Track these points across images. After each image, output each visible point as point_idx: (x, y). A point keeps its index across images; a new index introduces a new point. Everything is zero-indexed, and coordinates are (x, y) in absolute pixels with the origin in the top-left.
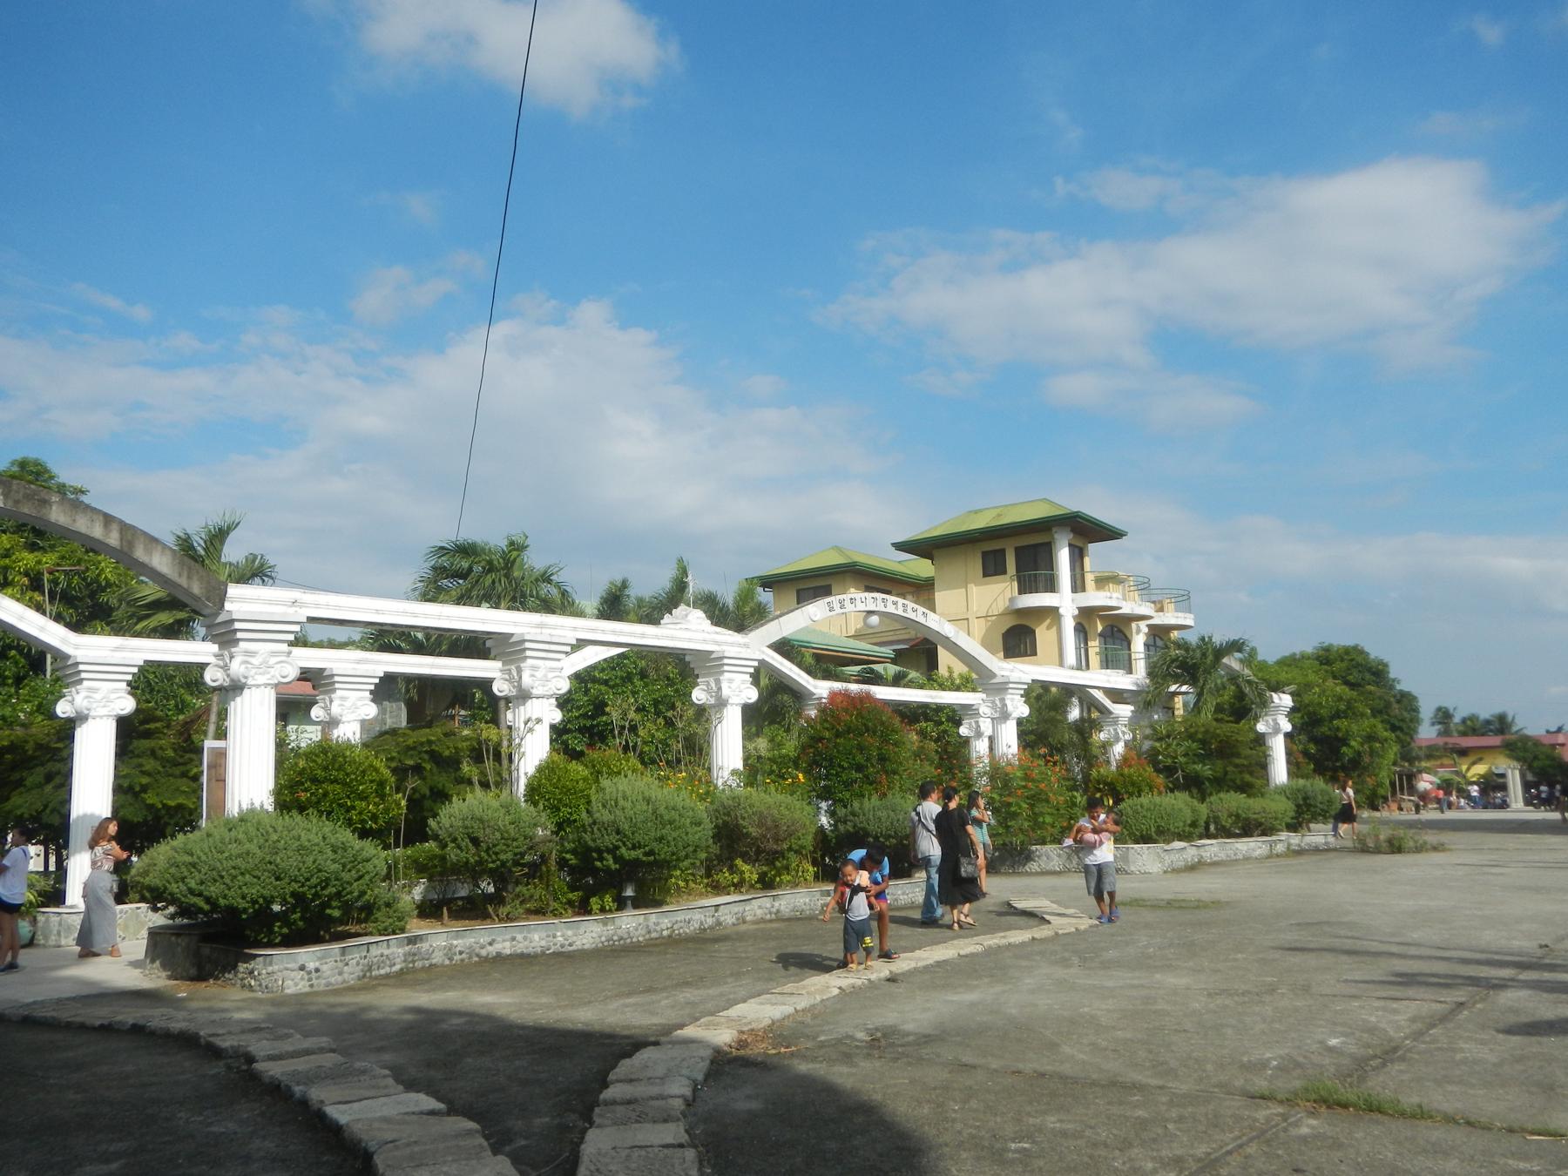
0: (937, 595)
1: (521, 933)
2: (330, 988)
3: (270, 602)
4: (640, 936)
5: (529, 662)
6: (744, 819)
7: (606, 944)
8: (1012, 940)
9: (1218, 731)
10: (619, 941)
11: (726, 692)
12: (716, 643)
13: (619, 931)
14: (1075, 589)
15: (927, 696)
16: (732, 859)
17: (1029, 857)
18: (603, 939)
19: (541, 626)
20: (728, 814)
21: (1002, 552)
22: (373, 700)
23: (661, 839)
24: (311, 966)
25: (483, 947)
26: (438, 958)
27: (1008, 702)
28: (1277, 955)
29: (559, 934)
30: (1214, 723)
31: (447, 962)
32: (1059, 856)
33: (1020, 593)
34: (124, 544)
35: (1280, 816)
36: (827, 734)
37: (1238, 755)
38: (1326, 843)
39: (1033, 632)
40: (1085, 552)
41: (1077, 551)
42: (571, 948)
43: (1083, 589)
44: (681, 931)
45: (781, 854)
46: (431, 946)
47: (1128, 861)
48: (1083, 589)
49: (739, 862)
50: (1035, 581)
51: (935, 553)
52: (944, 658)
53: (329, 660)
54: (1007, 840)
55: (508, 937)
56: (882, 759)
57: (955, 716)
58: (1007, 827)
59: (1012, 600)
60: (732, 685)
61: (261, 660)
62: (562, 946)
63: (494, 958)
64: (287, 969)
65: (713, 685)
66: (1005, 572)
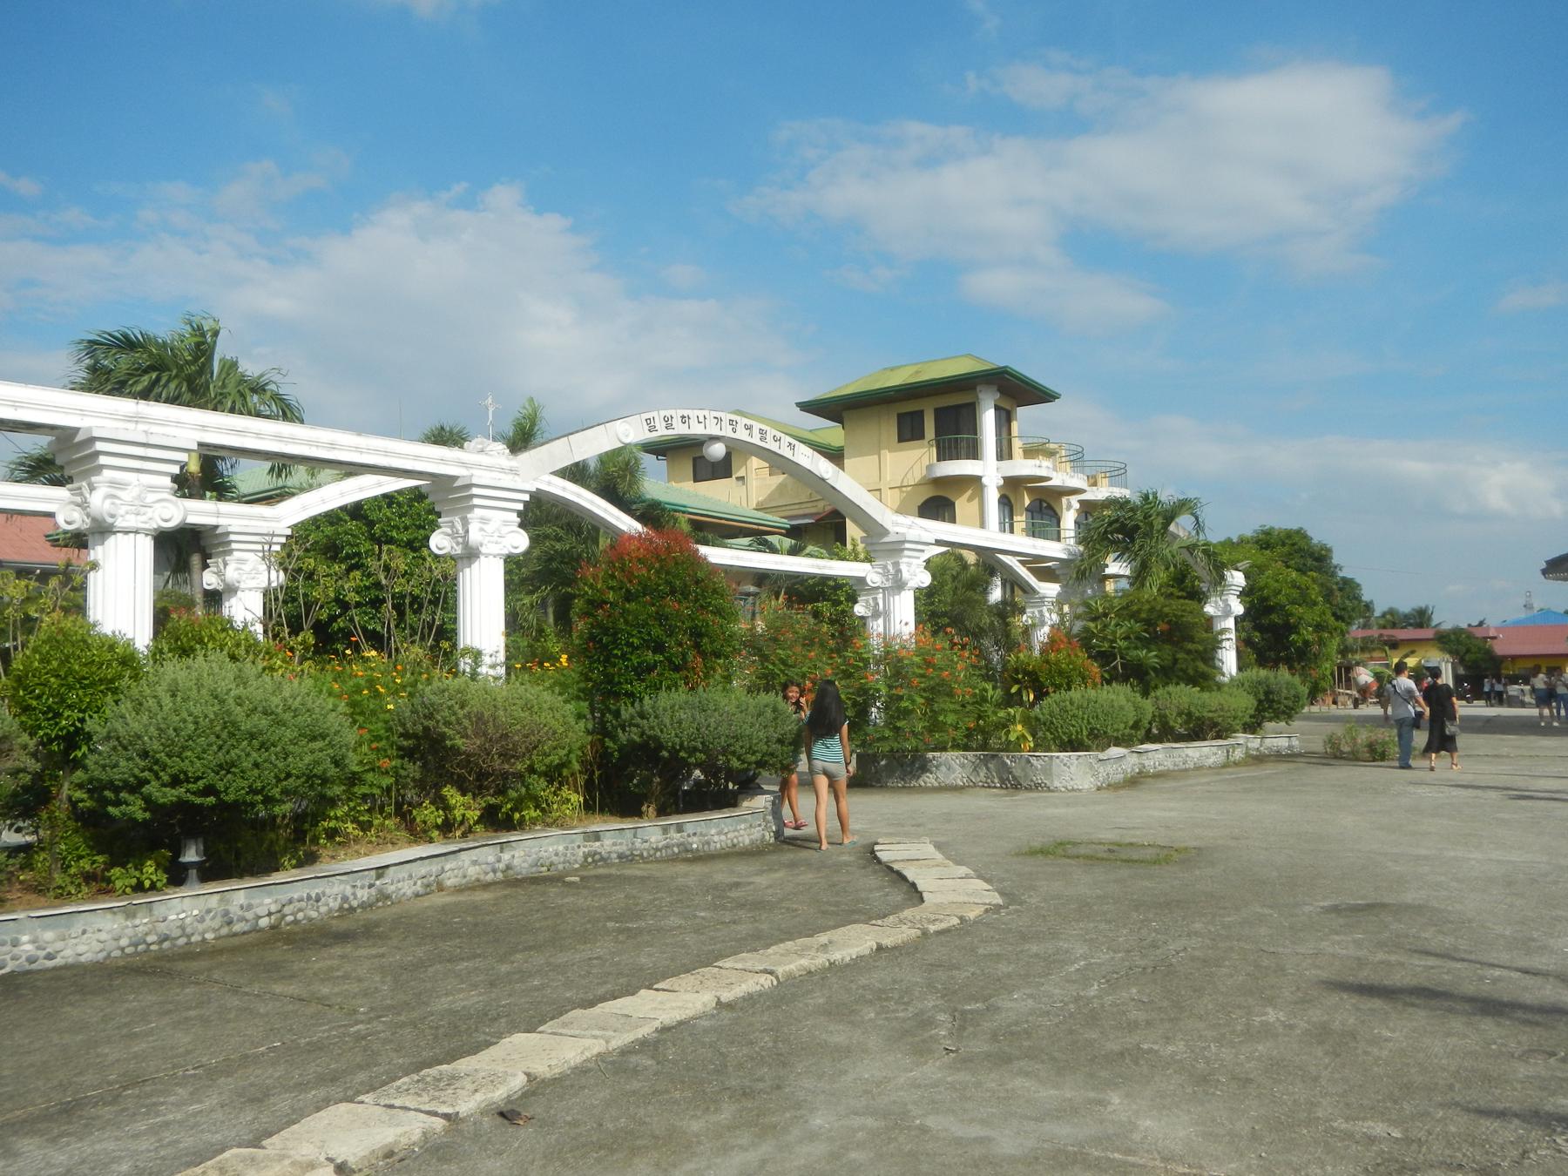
0: (846, 461)
5: (107, 473)
6: (448, 724)
7: (129, 950)
8: (837, 956)
9: (1166, 610)
10: (161, 942)
11: (475, 536)
12: (463, 464)
13: (162, 927)
14: (1000, 457)
15: (813, 566)
16: (438, 787)
17: (924, 768)
18: (124, 942)
19: (136, 419)
21: (920, 414)
23: (227, 767)
27: (903, 567)
28: (1344, 1012)
29: (25, 938)
30: (1161, 599)
32: (963, 766)
33: (938, 460)
35: (1240, 714)
36: (611, 596)
37: (1192, 640)
38: (1290, 747)
39: (954, 504)
40: (1013, 416)
41: (1004, 415)
42: (50, 964)
43: (1010, 457)
44: (300, 916)
47: (1051, 775)
48: (1010, 457)
49: (450, 792)
50: (956, 448)
51: (845, 414)
52: (853, 531)
54: (896, 745)
56: (697, 634)
57: (847, 591)
58: (897, 729)
59: (929, 467)
62: (32, 960)
65: (460, 528)
66: (922, 437)
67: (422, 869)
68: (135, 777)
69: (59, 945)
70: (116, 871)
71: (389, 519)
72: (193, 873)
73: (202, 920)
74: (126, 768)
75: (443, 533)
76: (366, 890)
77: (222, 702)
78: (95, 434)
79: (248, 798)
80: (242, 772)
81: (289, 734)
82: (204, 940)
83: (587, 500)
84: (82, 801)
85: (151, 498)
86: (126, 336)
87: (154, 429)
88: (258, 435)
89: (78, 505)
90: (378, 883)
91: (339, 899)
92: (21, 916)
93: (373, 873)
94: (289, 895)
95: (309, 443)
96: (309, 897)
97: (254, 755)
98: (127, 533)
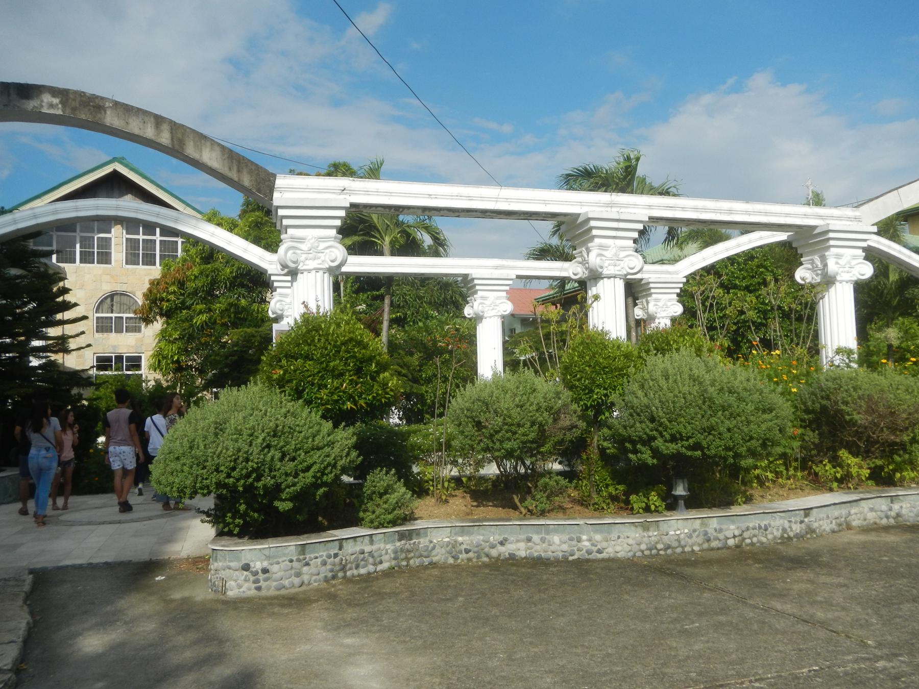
1: (538, 533)
2: (283, 592)
3: (319, 190)
4: (695, 545)
5: (597, 241)
6: (846, 403)
7: (647, 553)
10: (666, 549)
11: (832, 267)
12: (820, 217)
13: (665, 539)
16: (835, 450)
18: (643, 547)
19: (611, 205)
20: (828, 398)
22: (509, 299)
23: (710, 430)
24: (258, 565)
25: (493, 547)
26: (439, 556)
29: (584, 537)
31: (451, 561)
34: (175, 142)
42: (600, 556)
44: (755, 540)
45: (903, 446)
46: (431, 542)
49: (843, 454)
53: (472, 267)
55: (523, 537)
60: (840, 261)
61: (309, 245)
62: (589, 552)
63: (507, 559)
64: (230, 568)
67: (836, 512)
68: (646, 433)
69: (605, 544)
70: (633, 498)
71: (732, 273)
72: (682, 502)
73: (690, 537)
74: (641, 428)
75: (804, 268)
76: (799, 525)
77: (700, 383)
78: (590, 216)
79: (723, 453)
80: (720, 434)
81: (750, 407)
82: (693, 551)
83: (884, 245)
84: (609, 448)
85: (622, 254)
86: (586, 169)
87: (623, 210)
88: (683, 209)
89: (580, 263)
90: (806, 520)
91: (780, 531)
92: (581, 522)
93: (802, 512)
94: (747, 524)
95: (715, 211)
96: (760, 527)
97: (727, 422)
98: (609, 278)
